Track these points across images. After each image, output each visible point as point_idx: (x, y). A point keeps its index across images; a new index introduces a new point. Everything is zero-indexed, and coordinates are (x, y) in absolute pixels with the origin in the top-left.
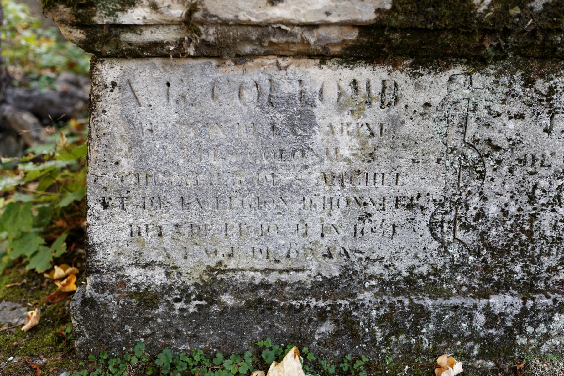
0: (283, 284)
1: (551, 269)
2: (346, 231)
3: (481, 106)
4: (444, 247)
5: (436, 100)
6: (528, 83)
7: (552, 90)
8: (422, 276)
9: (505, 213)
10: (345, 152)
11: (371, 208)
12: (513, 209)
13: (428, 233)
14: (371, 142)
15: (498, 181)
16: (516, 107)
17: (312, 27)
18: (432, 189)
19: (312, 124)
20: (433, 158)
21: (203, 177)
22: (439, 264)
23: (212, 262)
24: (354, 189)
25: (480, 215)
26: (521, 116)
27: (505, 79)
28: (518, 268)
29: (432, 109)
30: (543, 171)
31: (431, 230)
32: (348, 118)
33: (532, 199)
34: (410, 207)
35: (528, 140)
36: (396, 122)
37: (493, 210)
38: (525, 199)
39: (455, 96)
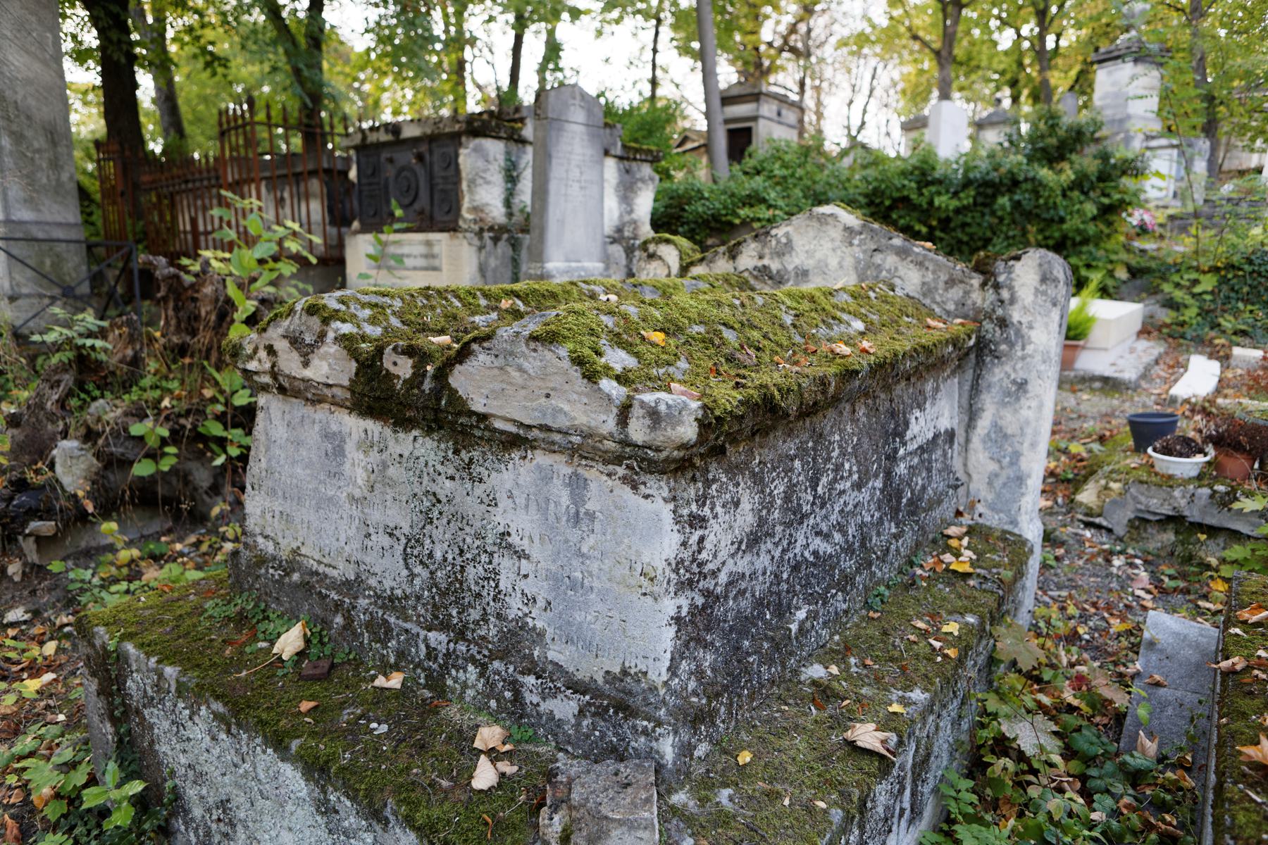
0: (326, 576)
1: (476, 623)
2: (355, 545)
3: (430, 464)
4: (412, 576)
5: (406, 454)
6: (456, 452)
7: (471, 460)
8: (397, 598)
9: (445, 560)
10: (360, 482)
11: (372, 530)
12: (450, 557)
13: (402, 562)
14: (373, 477)
15: (441, 529)
16: (451, 471)
17: (329, 386)
18: (403, 524)
19: (344, 456)
20: (404, 499)
21: (295, 481)
22: (408, 591)
23: (294, 545)
24: (363, 512)
25: (430, 556)
26: (452, 478)
27: (443, 446)
28: (454, 613)
29: (404, 460)
30: (468, 529)
31: (405, 560)
32: (362, 456)
33: (462, 552)
34: (391, 535)
35: (458, 500)
36: (385, 466)
37: (438, 555)
38: (457, 552)
39: (416, 453)
